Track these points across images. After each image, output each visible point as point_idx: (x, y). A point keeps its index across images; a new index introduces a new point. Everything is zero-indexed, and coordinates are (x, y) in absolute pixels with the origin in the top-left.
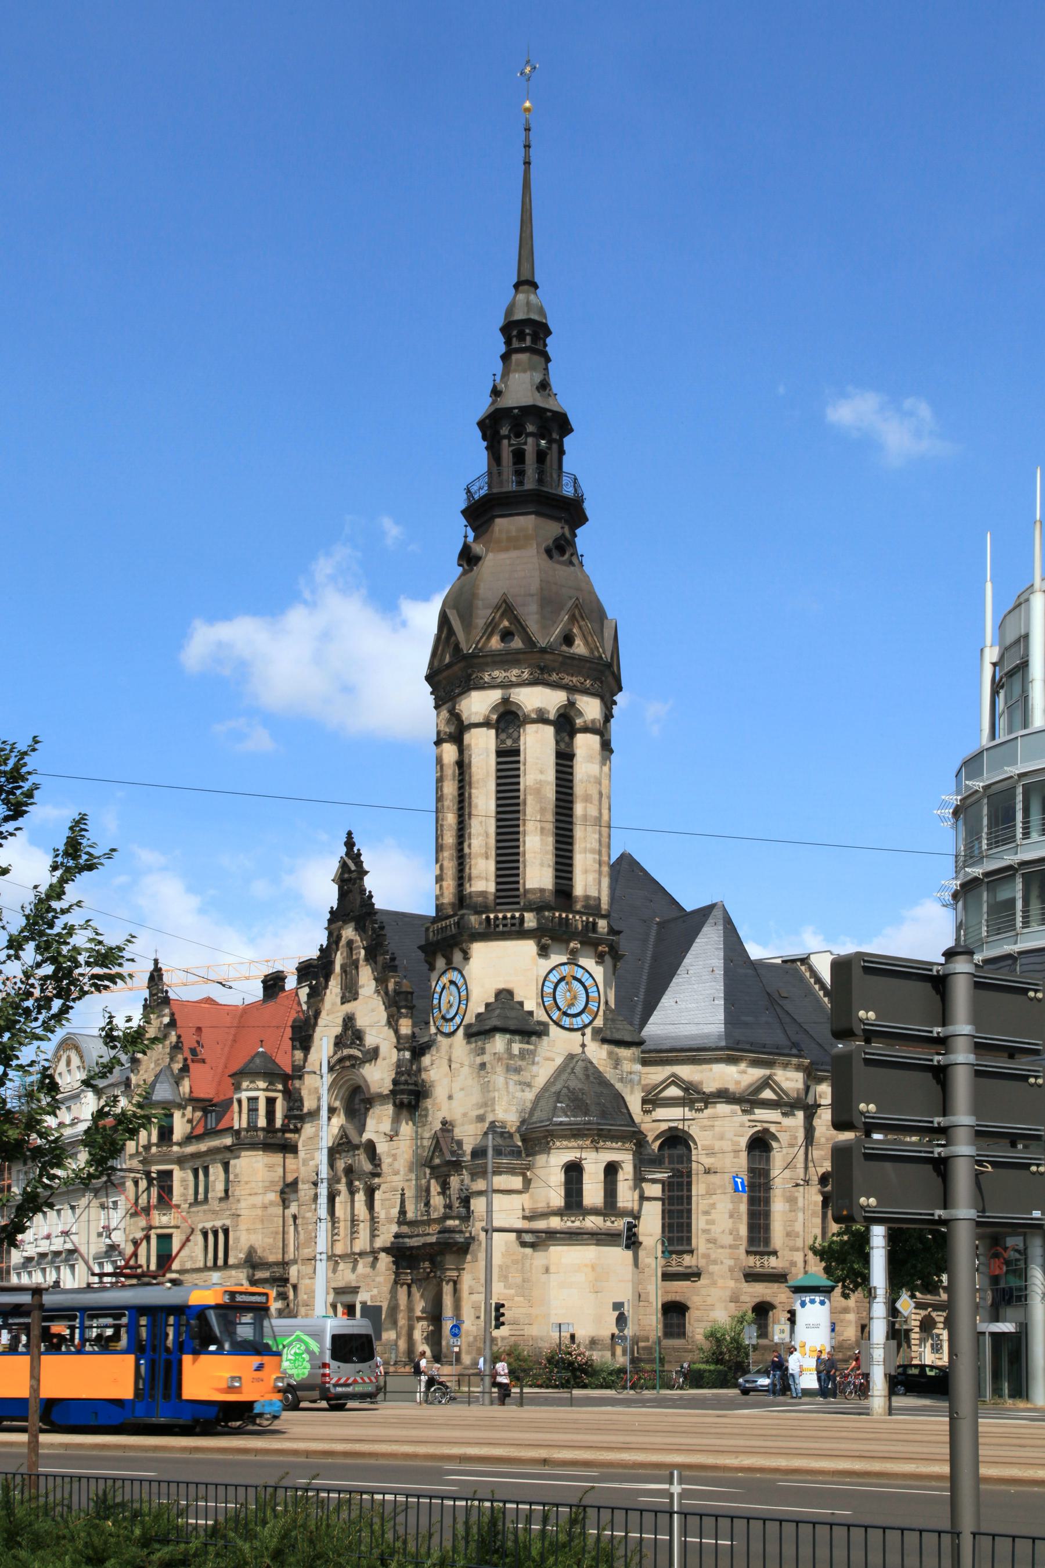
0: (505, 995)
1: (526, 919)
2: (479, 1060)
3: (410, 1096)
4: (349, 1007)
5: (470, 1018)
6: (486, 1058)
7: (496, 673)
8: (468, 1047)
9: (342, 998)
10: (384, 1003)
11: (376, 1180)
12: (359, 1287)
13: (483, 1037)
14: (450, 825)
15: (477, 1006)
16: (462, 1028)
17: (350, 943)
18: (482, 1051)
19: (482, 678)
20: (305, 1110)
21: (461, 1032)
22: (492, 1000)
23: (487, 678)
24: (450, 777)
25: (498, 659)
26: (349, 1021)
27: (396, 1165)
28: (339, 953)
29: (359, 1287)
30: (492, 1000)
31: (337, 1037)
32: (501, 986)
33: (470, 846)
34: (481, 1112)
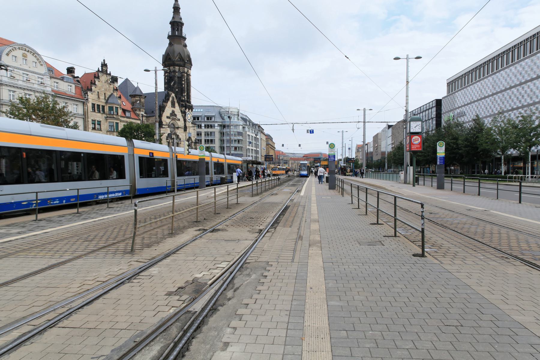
4: (173, 109)
26: (173, 112)
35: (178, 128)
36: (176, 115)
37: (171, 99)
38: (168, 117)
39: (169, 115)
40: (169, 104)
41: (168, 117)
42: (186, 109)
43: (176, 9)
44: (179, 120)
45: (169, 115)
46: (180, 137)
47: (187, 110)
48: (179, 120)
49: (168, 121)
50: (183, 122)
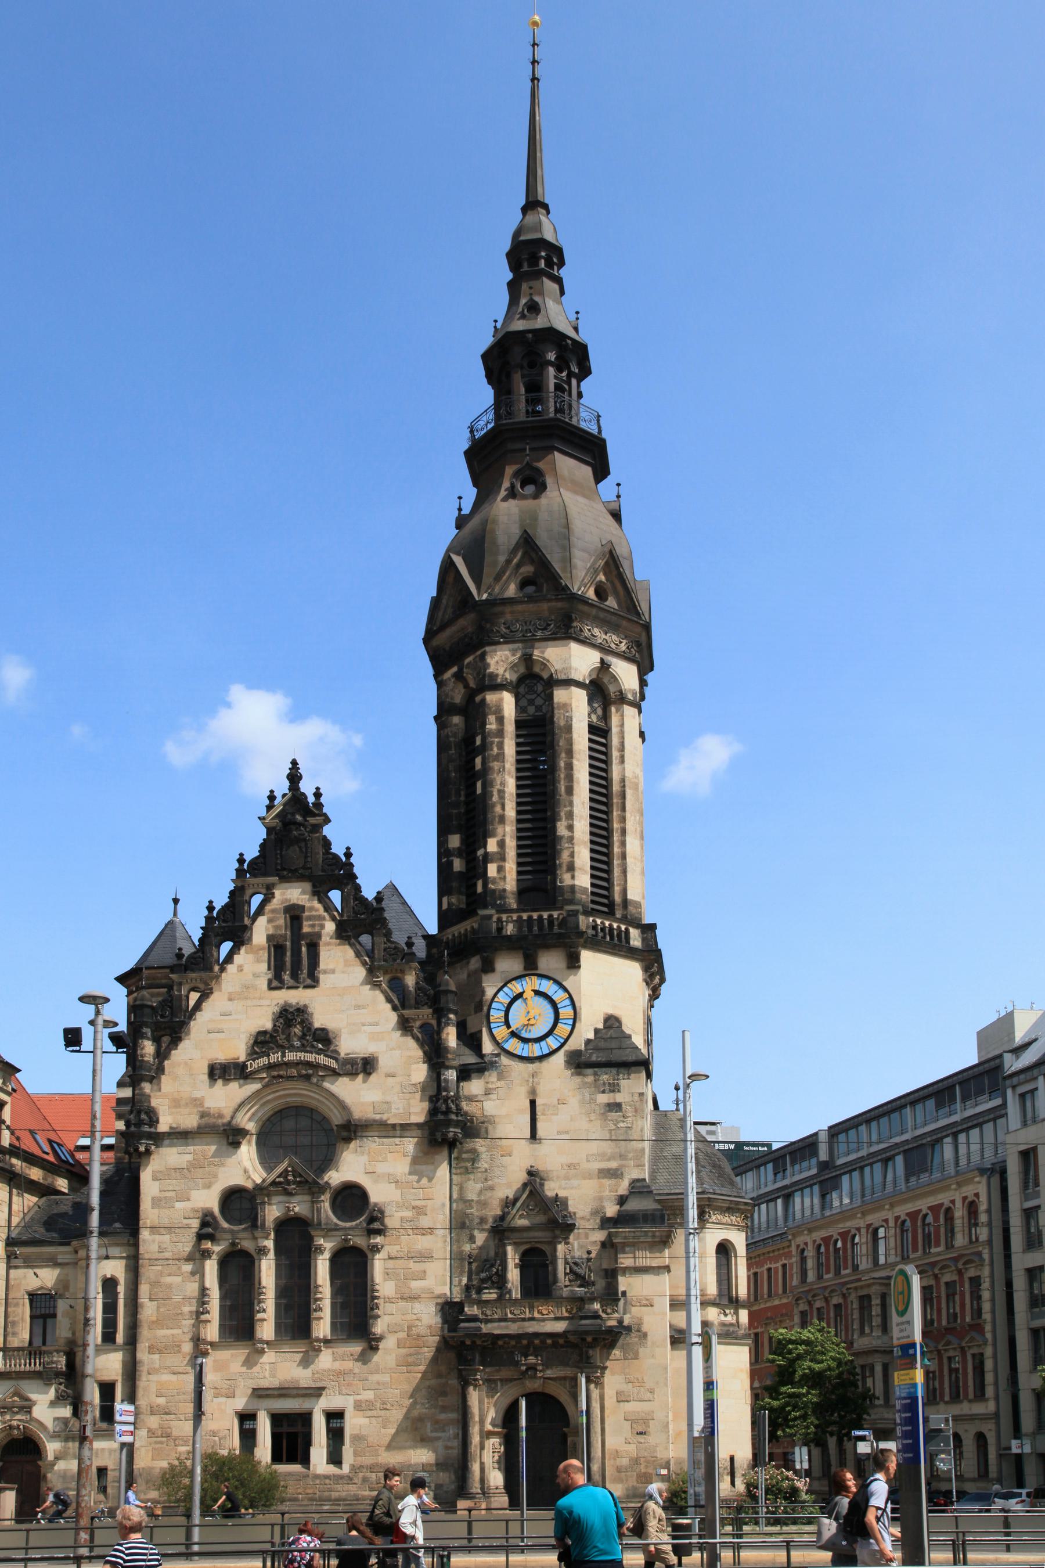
0: (612, 1022)
1: (632, 936)
2: (603, 1099)
3: (447, 1131)
4: (295, 997)
5: (577, 1043)
6: (619, 1098)
7: (596, 631)
8: (578, 1080)
9: (270, 982)
10: (389, 1000)
11: (378, 1240)
12: (323, 1388)
13: (614, 1071)
14: (511, 794)
15: (586, 1031)
16: (561, 1053)
17: (294, 914)
18: (614, 1088)
19: (581, 630)
20: (163, 1127)
21: (560, 1058)
22: (601, 1026)
23: (587, 633)
24: (509, 736)
25: (602, 615)
27: (425, 1222)
28: (262, 922)
29: (323, 1388)
30: (601, 1026)
31: (259, 1033)
32: (610, 1011)
33: (570, 828)
34: (613, 1165)
35: (352, 1130)
36: (324, 1039)
37: (261, 931)
38: (219, 1072)
39: (238, 1050)
40: (247, 968)
41: (219, 1072)
42: (488, 967)
43: (533, 260)
44: (366, 1066)
45: (238, 1050)
46: (377, 1194)
47: (508, 964)
48: (366, 1066)
49: (224, 1099)
50: (420, 1072)
